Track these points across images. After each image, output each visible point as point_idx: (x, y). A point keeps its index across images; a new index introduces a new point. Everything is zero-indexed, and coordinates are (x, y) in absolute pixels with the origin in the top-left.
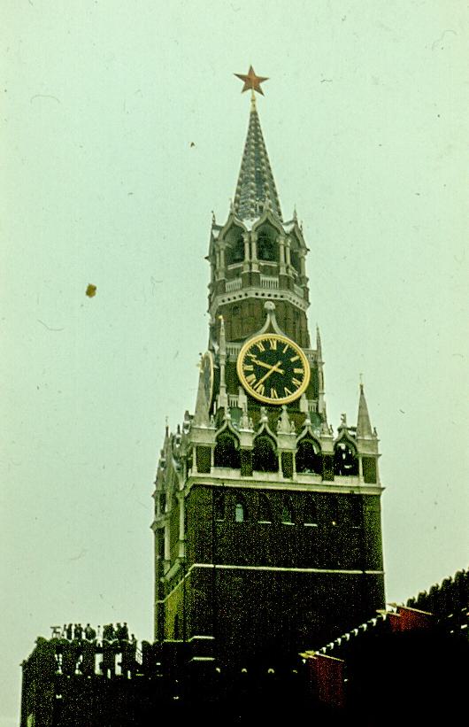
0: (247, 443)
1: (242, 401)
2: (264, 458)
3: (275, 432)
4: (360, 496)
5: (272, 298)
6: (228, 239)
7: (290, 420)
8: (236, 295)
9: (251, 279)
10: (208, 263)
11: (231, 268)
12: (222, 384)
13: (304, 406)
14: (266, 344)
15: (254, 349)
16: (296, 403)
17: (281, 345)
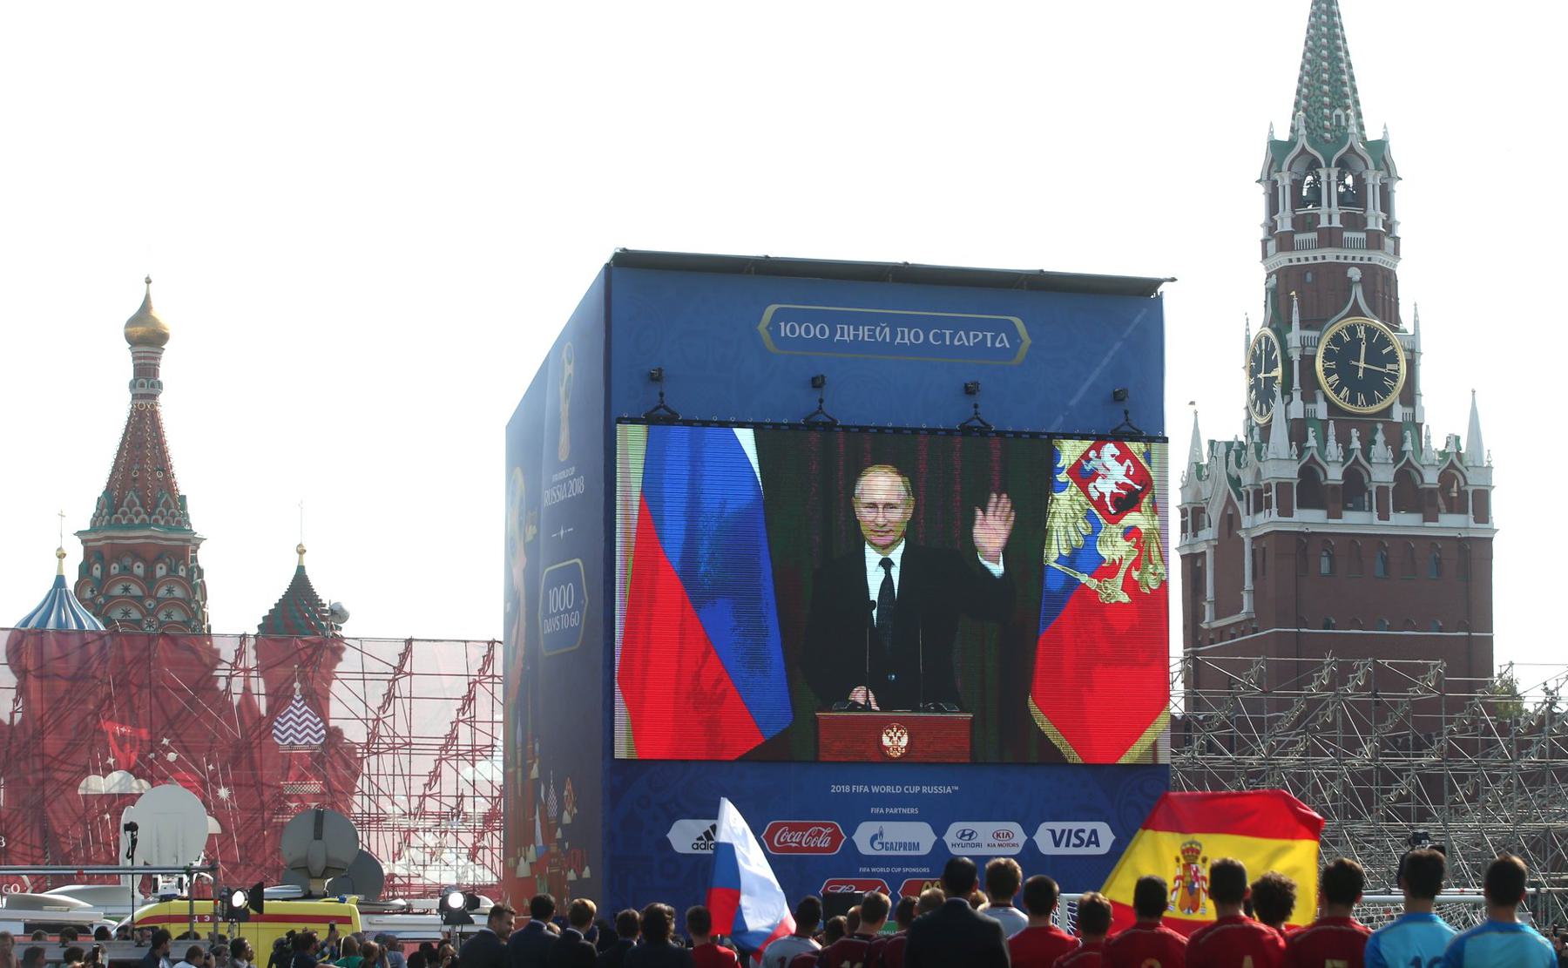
0: (1335, 474)
1: (1321, 411)
2: (1353, 491)
3: (1368, 460)
4: (1468, 539)
5: (1358, 261)
6: (1294, 168)
7: (1386, 443)
8: (1310, 254)
9: (1330, 238)
10: (1261, 189)
11: (1301, 212)
12: (1296, 384)
13: (1398, 414)
14: (1352, 330)
15: (1336, 339)
16: (1389, 409)
17: (1370, 331)
